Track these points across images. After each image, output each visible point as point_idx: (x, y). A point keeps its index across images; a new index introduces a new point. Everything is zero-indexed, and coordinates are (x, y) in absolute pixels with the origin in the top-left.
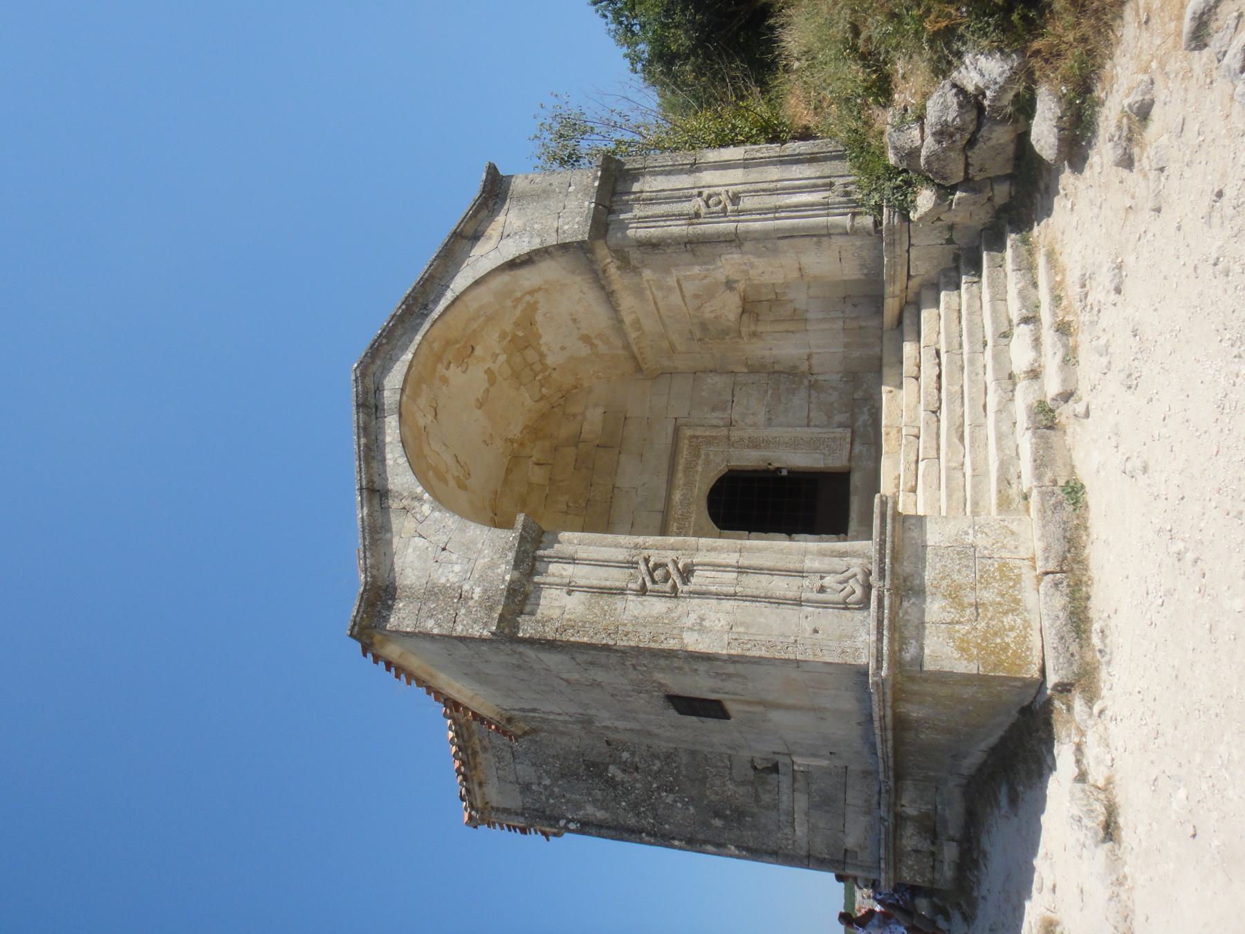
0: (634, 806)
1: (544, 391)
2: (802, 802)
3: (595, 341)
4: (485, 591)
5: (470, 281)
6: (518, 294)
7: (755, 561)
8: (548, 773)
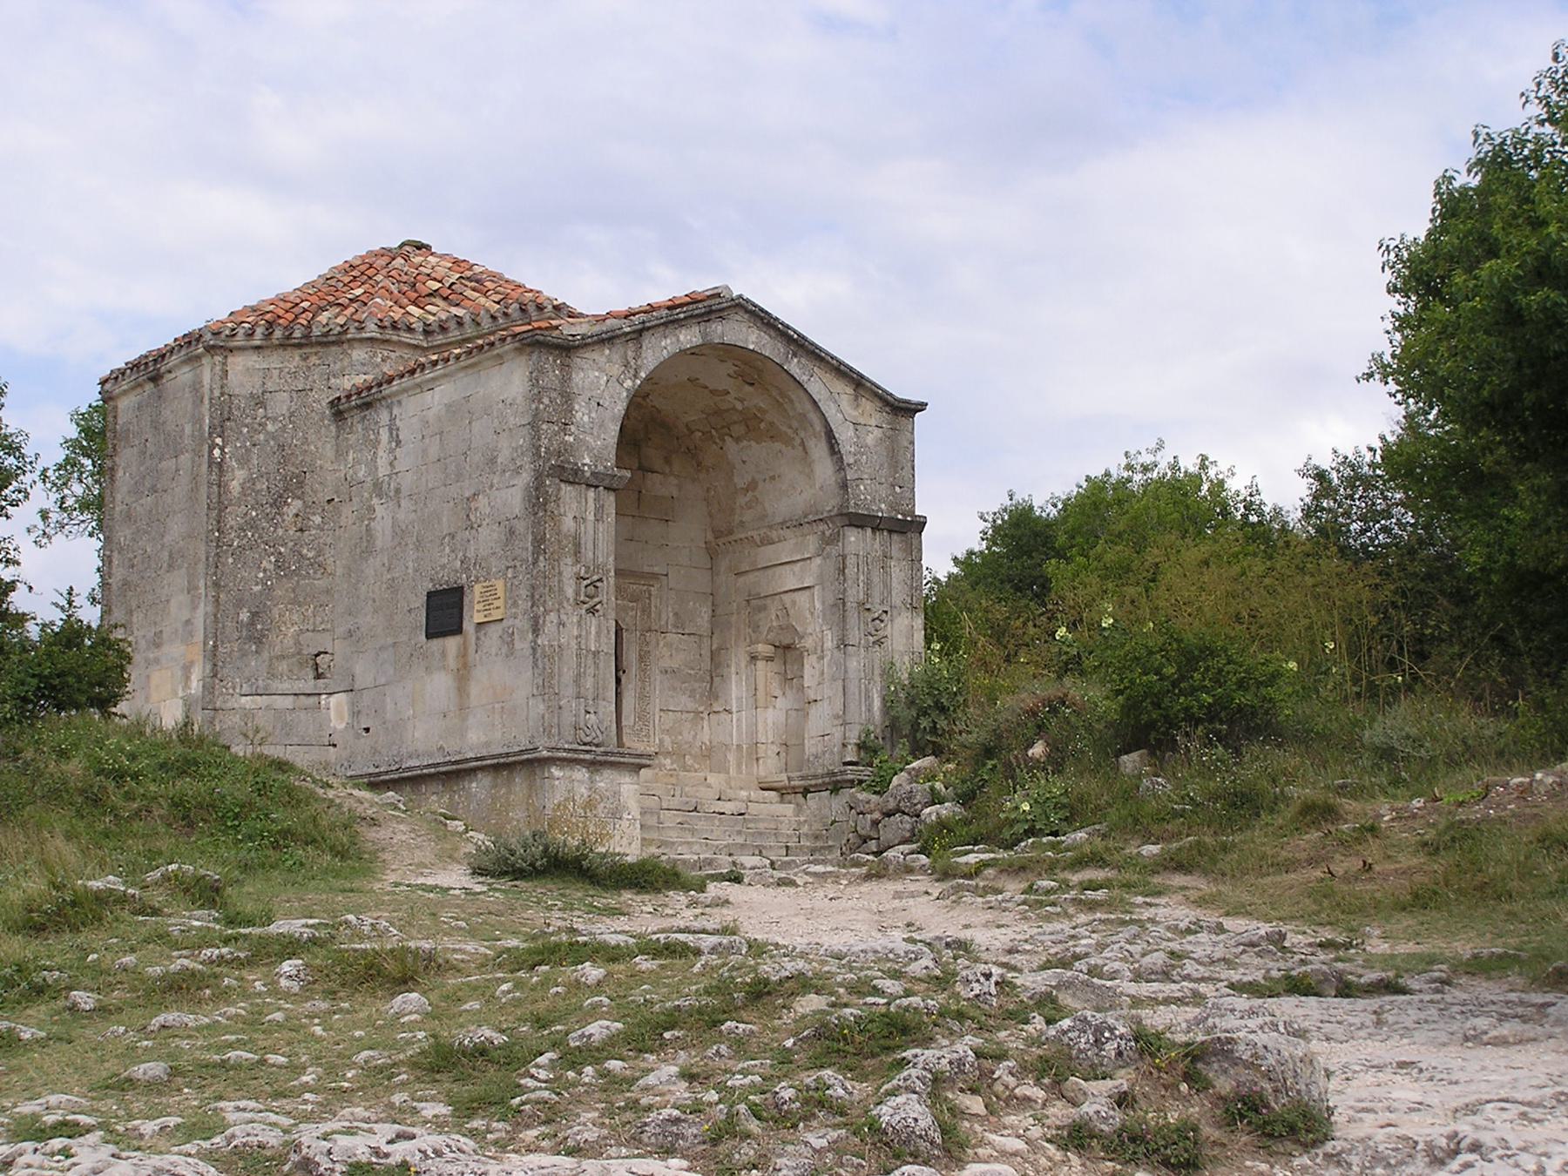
0: (252, 525)
3: (750, 494)
4: (571, 445)
6: (802, 434)
7: (601, 665)
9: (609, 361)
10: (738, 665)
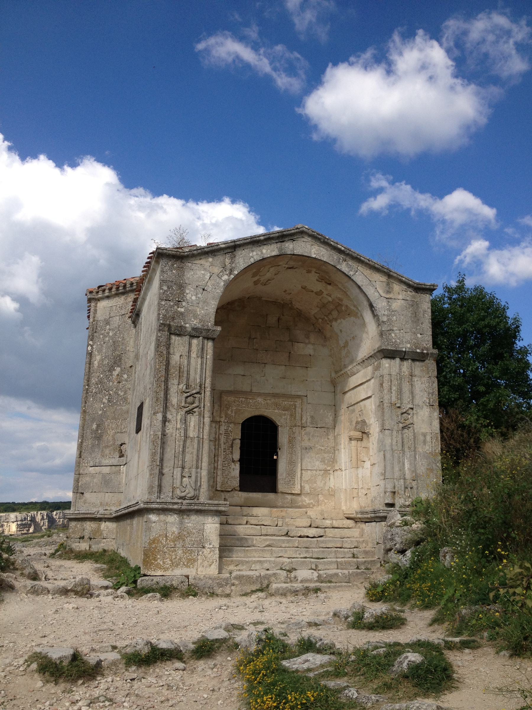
0: (101, 382)
1: (320, 320)
2: (106, 470)
3: (346, 349)
4: (182, 314)
5: (360, 283)
8: (115, 334)
9: (212, 265)
10: (344, 443)
